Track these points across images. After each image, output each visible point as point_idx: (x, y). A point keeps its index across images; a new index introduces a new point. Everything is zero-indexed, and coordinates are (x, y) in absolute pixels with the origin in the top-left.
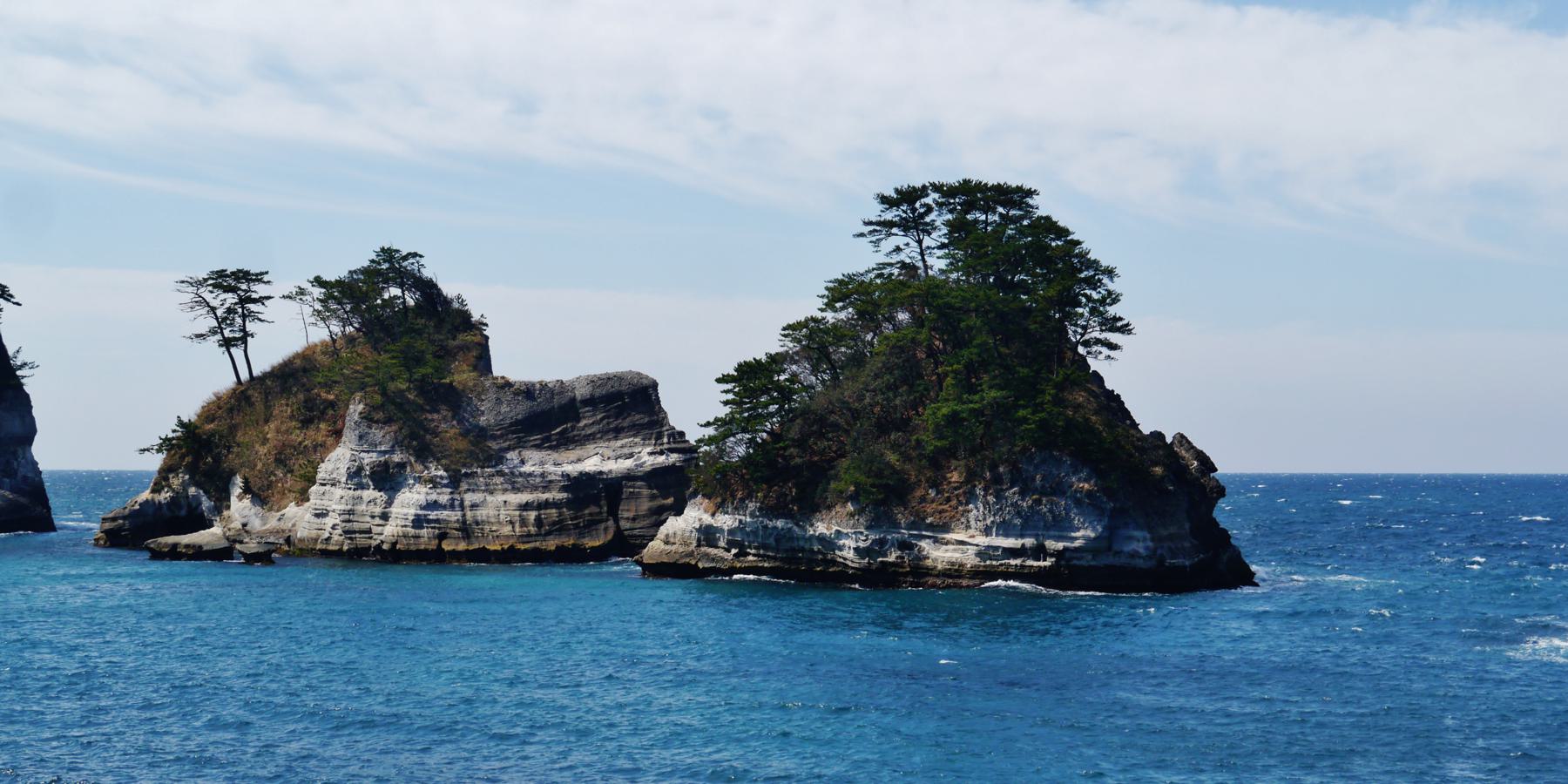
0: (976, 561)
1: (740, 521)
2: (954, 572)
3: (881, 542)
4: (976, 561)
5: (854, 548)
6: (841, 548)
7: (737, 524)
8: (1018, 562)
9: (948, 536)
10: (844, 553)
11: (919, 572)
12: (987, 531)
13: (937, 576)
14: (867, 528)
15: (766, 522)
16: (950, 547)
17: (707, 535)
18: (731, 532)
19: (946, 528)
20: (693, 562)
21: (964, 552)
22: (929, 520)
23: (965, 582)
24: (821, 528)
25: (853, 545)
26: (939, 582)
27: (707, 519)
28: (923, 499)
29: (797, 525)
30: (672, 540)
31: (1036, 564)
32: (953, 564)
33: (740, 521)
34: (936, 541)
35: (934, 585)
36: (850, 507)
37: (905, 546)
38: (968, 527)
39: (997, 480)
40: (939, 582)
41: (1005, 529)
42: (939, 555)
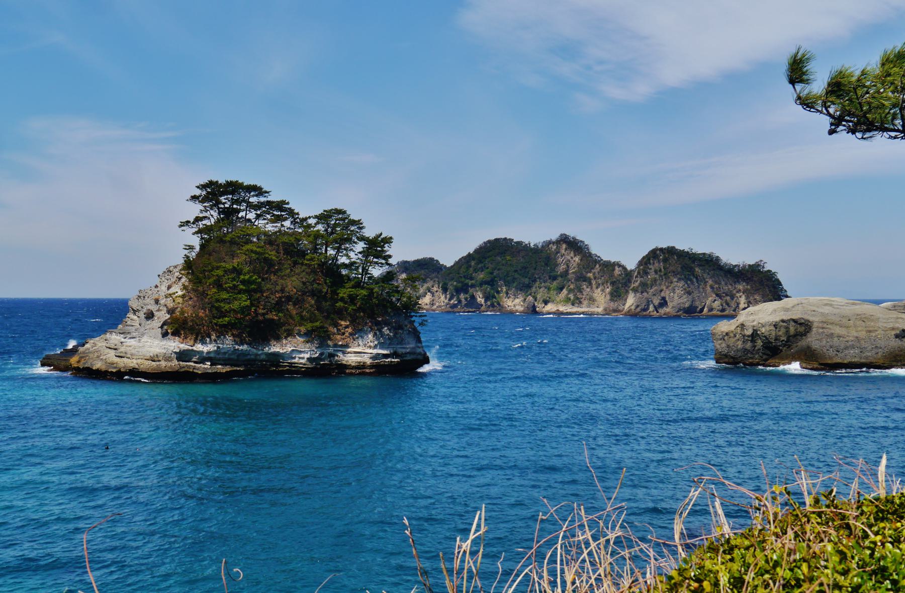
0: (371, 361)
1: (218, 347)
2: (361, 366)
3: (321, 354)
4: (371, 361)
5: (308, 358)
6: (294, 358)
7: (216, 348)
8: (389, 360)
9: (349, 350)
10: (293, 361)
11: (342, 369)
12: (375, 347)
13: (352, 369)
14: (317, 348)
15: (237, 347)
16: (349, 355)
17: (182, 356)
18: (208, 353)
19: (347, 346)
20: (191, 370)
21: (361, 357)
22: (340, 343)
23: (367, 371)
24: (275, 348)
25: (307, 356)
26: (354, 371)
27: (184, 347)
28: (334, 334)
29: (253, 348)
30: (156, 359)
31: (396, 360)
32: (360, 362)
33: (218, 347)
34: (344, 353)
35: (351, 374)
36: (301, 339)
37: (332, 356)
38: (359, 345)
39: (378, 324)
40: (354, 371)
41: (382, 345)
42: (350, 358)
